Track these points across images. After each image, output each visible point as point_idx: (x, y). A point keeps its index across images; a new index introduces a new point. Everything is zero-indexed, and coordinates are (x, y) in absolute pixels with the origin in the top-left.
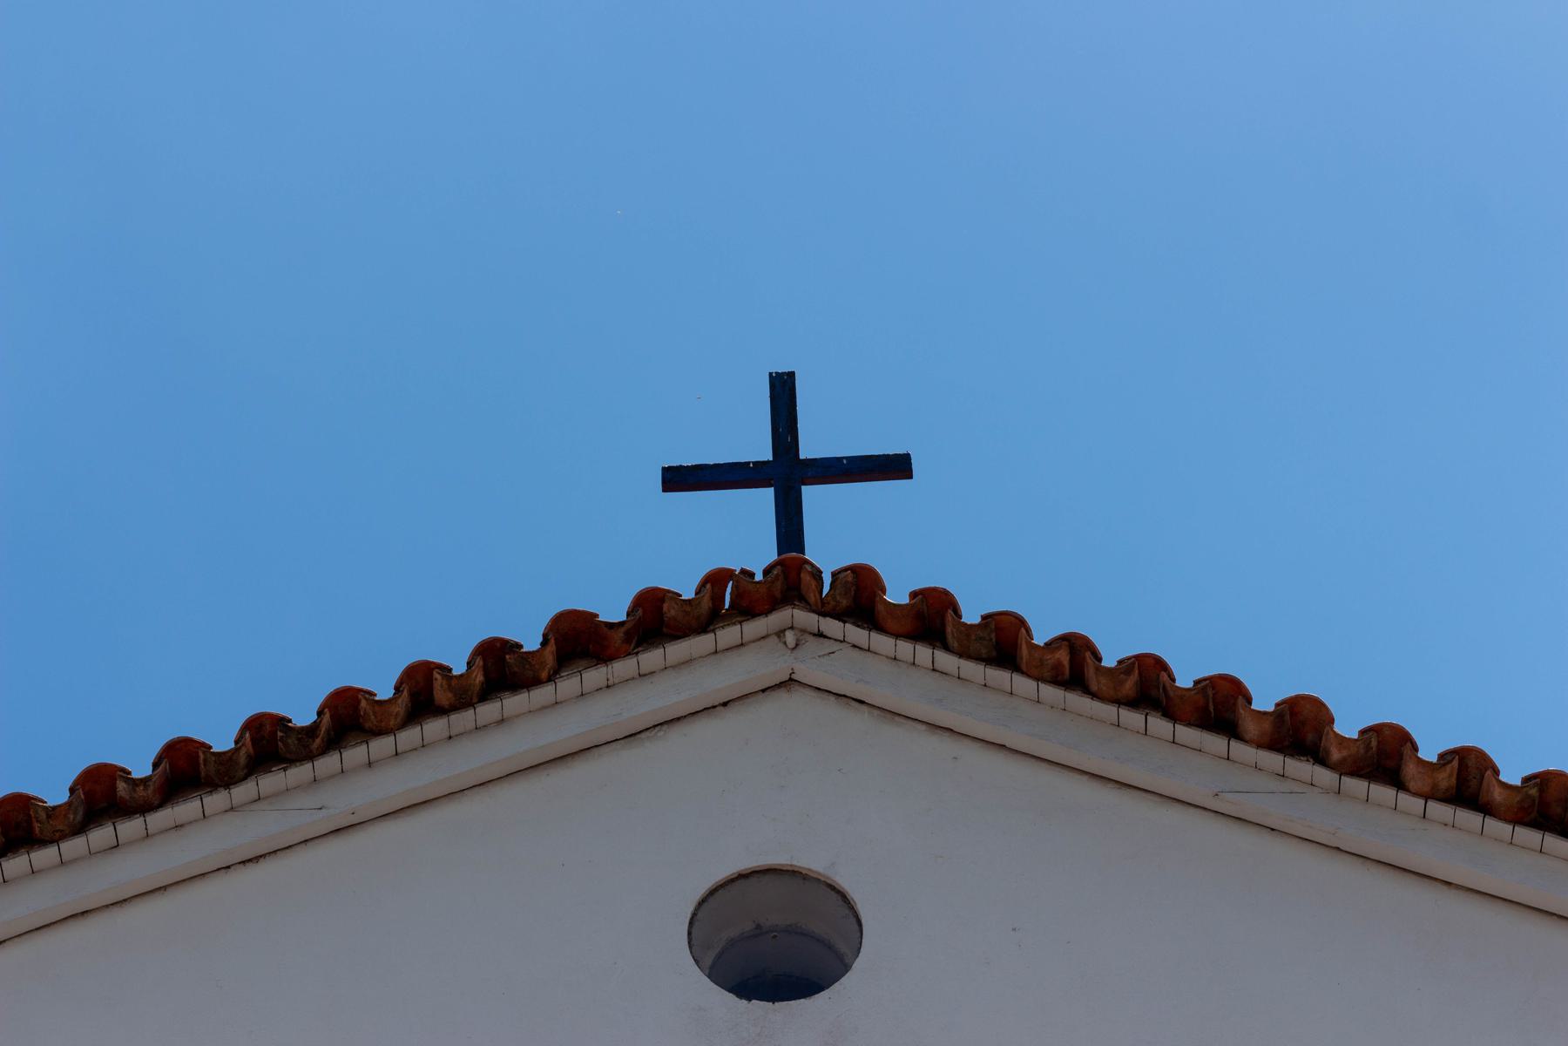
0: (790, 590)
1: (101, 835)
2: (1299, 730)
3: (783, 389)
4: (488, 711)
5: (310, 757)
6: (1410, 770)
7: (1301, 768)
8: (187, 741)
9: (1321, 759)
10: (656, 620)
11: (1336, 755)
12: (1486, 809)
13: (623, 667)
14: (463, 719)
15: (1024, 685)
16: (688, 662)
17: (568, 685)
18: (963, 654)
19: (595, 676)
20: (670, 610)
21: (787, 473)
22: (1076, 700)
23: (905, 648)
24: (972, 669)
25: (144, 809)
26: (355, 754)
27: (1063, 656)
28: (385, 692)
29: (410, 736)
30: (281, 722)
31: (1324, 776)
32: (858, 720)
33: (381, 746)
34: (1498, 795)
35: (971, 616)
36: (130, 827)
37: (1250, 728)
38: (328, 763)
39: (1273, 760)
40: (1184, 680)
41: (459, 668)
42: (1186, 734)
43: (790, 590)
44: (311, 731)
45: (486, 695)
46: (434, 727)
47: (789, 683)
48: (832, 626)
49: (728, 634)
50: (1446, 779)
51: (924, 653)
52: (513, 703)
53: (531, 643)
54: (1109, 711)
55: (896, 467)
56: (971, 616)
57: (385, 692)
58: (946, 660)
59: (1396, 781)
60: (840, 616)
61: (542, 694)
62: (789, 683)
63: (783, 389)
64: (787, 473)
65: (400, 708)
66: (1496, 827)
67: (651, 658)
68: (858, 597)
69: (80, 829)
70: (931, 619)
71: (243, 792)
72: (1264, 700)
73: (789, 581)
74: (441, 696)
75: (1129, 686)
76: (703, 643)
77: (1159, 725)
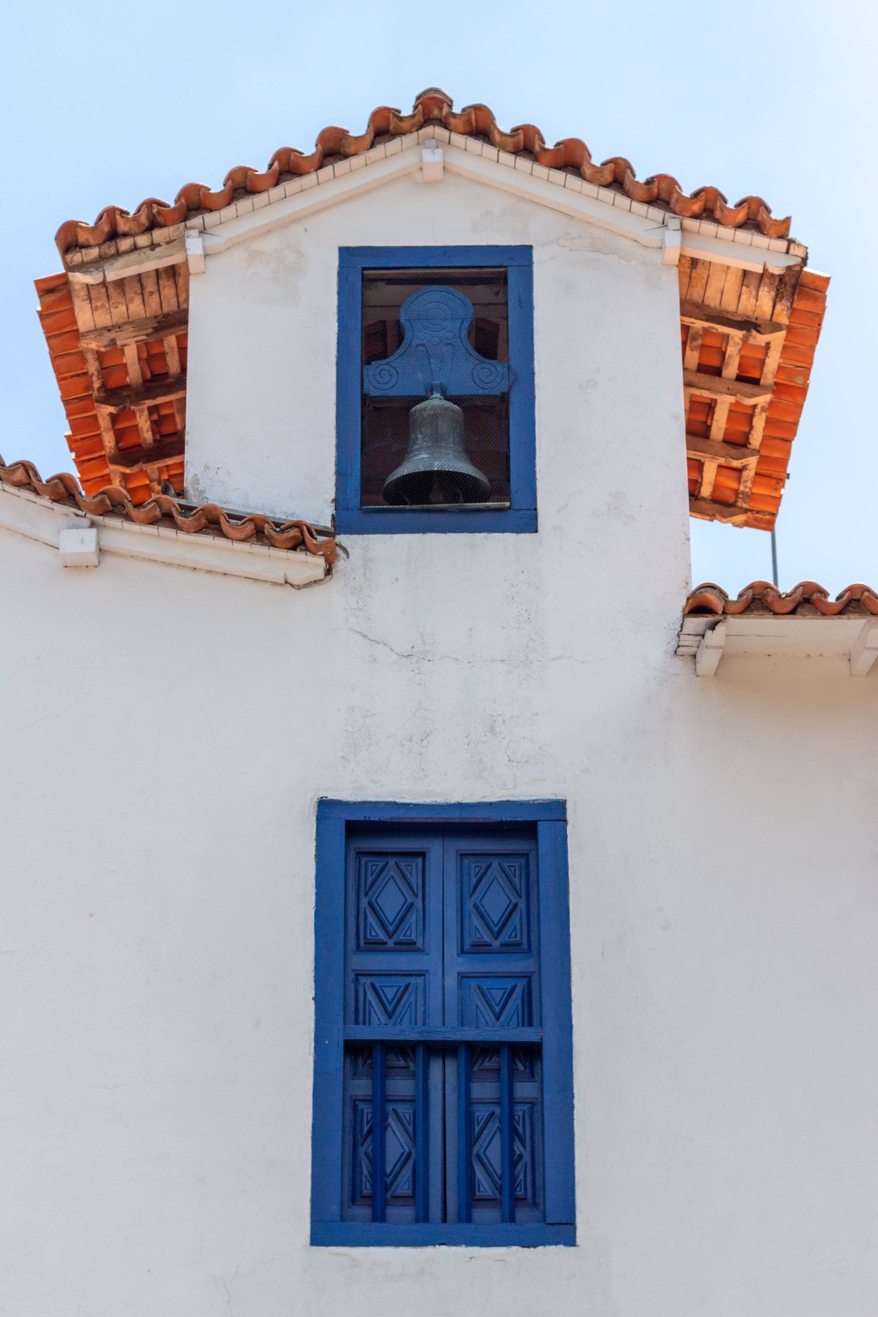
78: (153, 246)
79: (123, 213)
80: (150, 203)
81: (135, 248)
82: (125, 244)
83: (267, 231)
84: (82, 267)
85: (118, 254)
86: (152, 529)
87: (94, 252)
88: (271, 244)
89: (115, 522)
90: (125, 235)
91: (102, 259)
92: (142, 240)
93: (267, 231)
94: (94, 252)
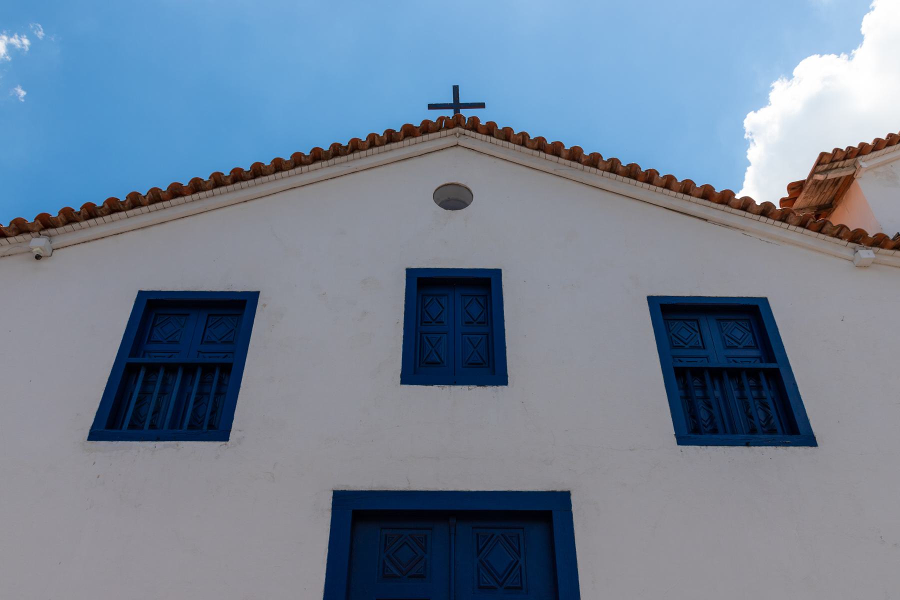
0: (457, 120)
1: (298, 170)
2: (575, 155)
3: (456, 89)
4: (388, 147)
5: (346, 154)
6: (600, 163)
7: (575, 164)
8: (318, 148)
9: (579, 161)
10: (427, 128)
11: (583, 160)
12: (617, 173)
13: (419, 139)
14: (382, 148)
15: (511, 145)
16: (434, 139)
17: (406, 142)
18: (498, 138)
19: (412, 140)
20: (430, 126)
21: (456, 105)
22: (524, 149)
23: (484, 136)
24: (500, 142)
25: (308, 164)
26: (357, 155)
27: (521, 137)
28: (364, 139)
29: (369, 151)
30: (340, 145)
31: (580, 166)
32: (474, 153)
33: (363, 153)
34: (620, 169)
35: (500, 128)
36: (305, 168)
37: (564, 154)
38: (351, 156)
39: (568, 162)
40: (549, 142)
41: (381, 135)
42: (549, 156)
43: (457, 120)
44: (347, 147)
45: (388, 142)
46: (375, 150)
47: (457, 145)
48: (467, 132)
49: (443, 133)
50: (608, 166)
51: (488, 138)
52: (394, 145)
53: (398, 130)
54: (530, 151)
55: (481, 105)
56: (500, 128)
57: (364, 139)
58: (494, 140)
59: (597, 167)
60: (470, 129)
61: (400, 144)
62: (457, 145)
63: (456, 89)
64: (456, 105)
65: (368, 144)
66: (620, 177)
67: (425, 137)
68: (474, 126)
69: (293, 168)
70: (490, 130)
71: (331, 162)
72: (567, 147)
73: (457, 121)
74: (377, 142)
75: (536, 145)
76: (437, 134)
77: (542, 154)
78: (843, 167)
79: (841, 150)
80: (849, 148)
81: (837, 168)
82: (836, 164)
83: (878, 166)
84: (820, 173)
85: (831, 169)
86: (892, 252)
87: (826, 166)
88: (880, 170)
89: (877, 249)
90: (837, 161)
91: (826, 171)
92: (841, 164)
93: (878, 166)
94: (826, 166)
